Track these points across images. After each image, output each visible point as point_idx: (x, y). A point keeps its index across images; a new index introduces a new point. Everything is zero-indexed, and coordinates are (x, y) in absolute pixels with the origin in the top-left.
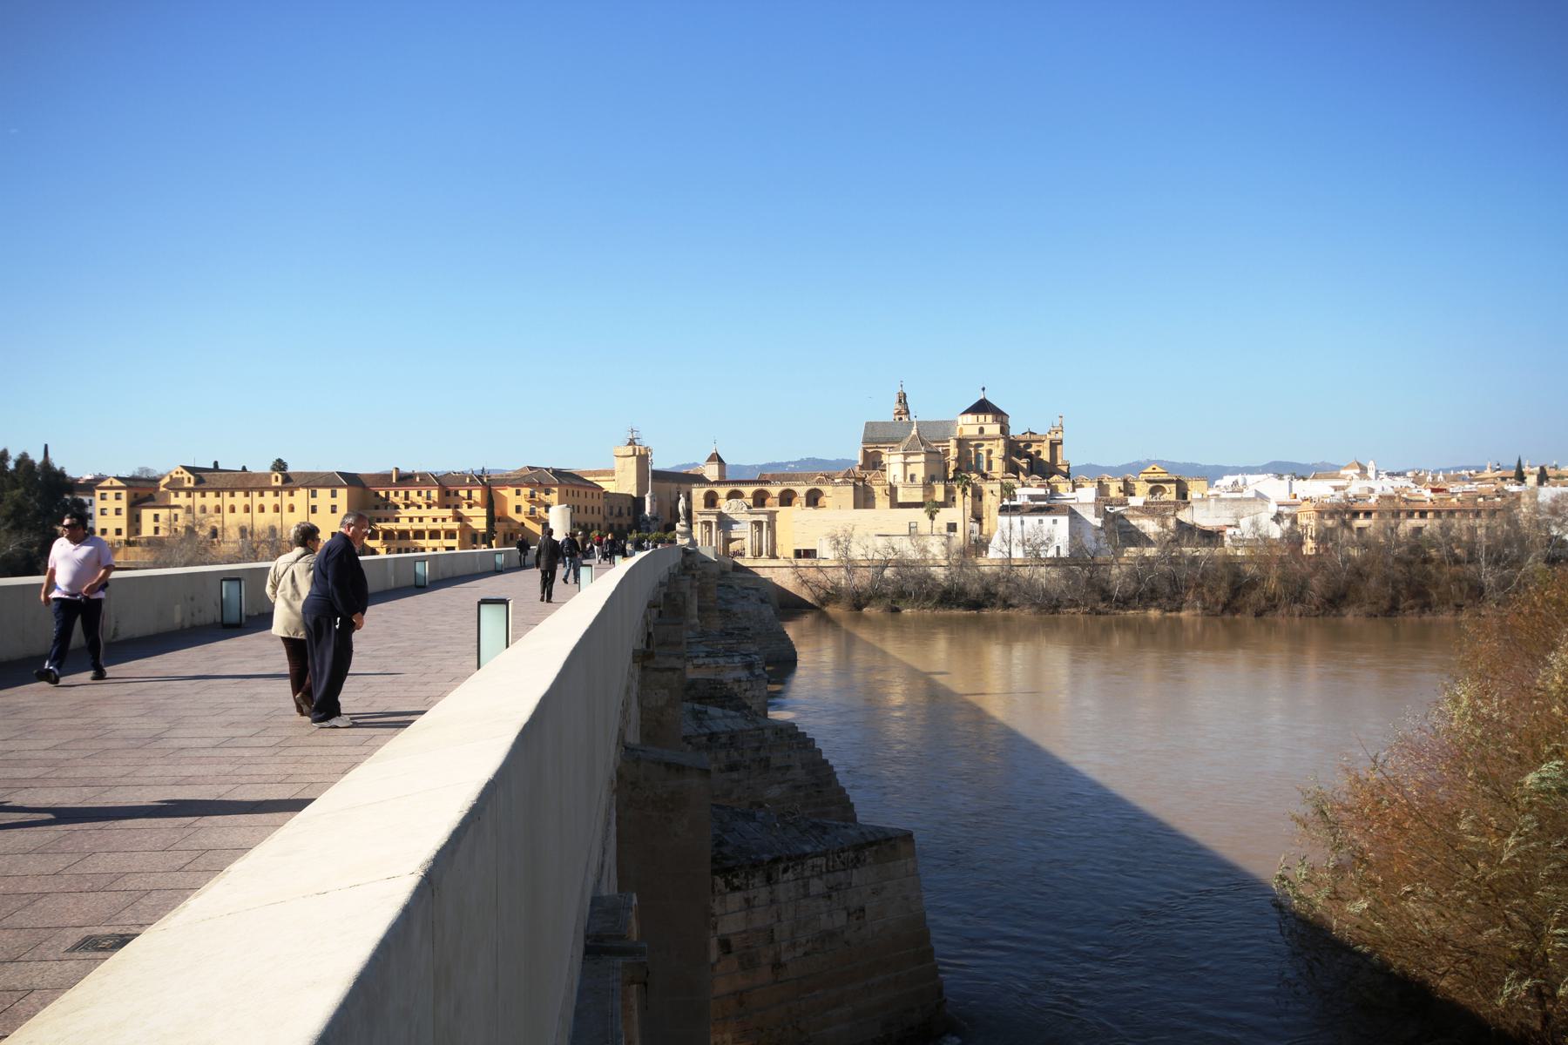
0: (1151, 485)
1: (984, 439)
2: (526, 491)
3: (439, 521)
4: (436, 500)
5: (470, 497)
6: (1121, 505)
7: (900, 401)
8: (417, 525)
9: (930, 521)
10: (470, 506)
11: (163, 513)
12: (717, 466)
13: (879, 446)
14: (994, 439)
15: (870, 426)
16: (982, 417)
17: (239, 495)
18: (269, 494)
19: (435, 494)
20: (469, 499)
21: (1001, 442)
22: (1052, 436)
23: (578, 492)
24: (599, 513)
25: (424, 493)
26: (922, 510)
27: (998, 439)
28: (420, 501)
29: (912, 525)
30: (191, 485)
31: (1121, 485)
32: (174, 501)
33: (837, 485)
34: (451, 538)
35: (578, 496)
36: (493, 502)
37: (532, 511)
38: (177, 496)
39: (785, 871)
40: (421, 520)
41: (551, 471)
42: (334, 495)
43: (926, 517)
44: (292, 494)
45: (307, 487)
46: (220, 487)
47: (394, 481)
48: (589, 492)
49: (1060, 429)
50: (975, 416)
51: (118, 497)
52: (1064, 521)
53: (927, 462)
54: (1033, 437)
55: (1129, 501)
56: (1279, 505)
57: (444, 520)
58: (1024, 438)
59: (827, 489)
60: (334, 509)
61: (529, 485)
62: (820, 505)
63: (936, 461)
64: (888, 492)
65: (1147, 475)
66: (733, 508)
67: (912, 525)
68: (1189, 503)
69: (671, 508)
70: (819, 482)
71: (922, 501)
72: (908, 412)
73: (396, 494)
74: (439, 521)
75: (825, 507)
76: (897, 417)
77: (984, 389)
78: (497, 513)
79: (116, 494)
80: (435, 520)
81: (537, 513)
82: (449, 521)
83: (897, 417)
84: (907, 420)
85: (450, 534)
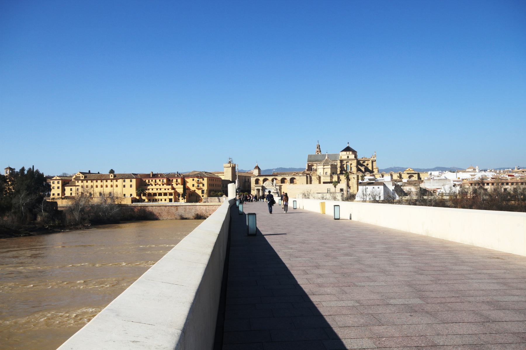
0: (409, 175)
1: (349, 160)
3: (167, 189)
4: (166, 182)
5: (177, 181)
6: (400, 182)
7: (318, 148)
8: (159, 191)
9: (335, 188)
10: (177, 185)
11: (74, 188)
12: (258, 170)
13: (313, 163)
14: (353, 160)
15: (310, 156)
16: (348, 153)
17: (99, 181)
18: (109, 181)
19: (165, 180)
20: (176, 182)
21: (355, 161)
22: (372, 159)
23: (213, 179)
24: (220, 187)
25: (161, 180)
26: (331, 185)
27: (354, 160)
28: (160, 183)
29: (328, 189)
30: (83, 178)
31: (399, 175)
32: (77, 184)
33: (300, 176)
34: (171, 196)
35: (213, 181)
37: (198, 186)
38: (78, 182)
40: (160, 189)
41: (204, 172)
42: (131, 181)
43: (333, 186)
44: (117, 181)
45: (122, 179)
46: (93, 179)
47: (151, 176)
49: (375, 156)
50: (346, 152)
51: (58, 183)
52: (382, 187)
53: (331, 168)
54: (366, 159)
55: (403, 181)
56: (453, 181)
57: (168, 189)
58: (362, 159)
60: (131, 186)
61: (198, 177)
62: (295, 183)
63: (334, 168)
64: (318, 178)
65: (407, 171)
66: (267, 184)
67: (328, 189)
68: (423, 181)
69: (243, 185)
70: (294, 175)
71: (330, 181)
72: (320, 151)
73: (152, 181)
74: (167, 189)
75: (296, 183)
76: (317, 153)
77: (348, 143)
78: (186, 187)
79: (58, 182)
80: (165, 189)
81: (200, 187)
82: (170, 189)
83: (317, 153)
84: (320, 154)
85: (171, 194)
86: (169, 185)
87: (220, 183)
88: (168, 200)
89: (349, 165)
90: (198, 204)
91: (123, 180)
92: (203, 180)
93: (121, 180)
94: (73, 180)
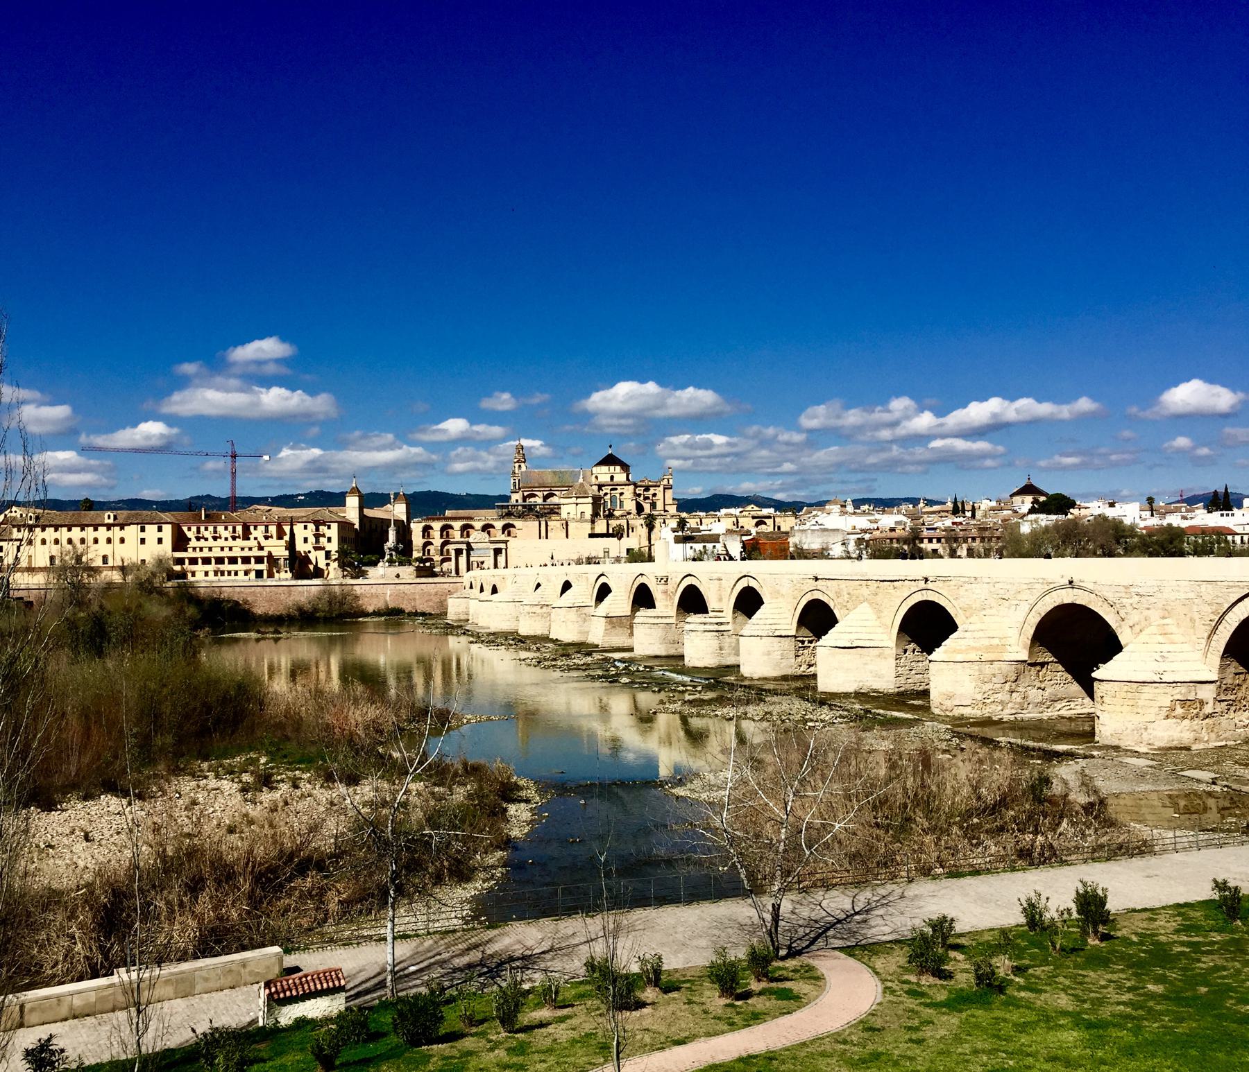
3: (247, 549)
4: (241, 533)
16: (612, 468)
17: (76, 530)
19: (239, 529)
25: (230, 528)
42: (160, 529)
45: (138, 524)
57: (250, 549)
59: (518, 523)
60: (160, 541)
73: (206, 529)
76: (517, 465)
80: (243, 549)
83: (517, 465)
85: (259, 560)
88: (253, 575)
89: (618, 495)
90: (360, 581)
92: (329, 527)
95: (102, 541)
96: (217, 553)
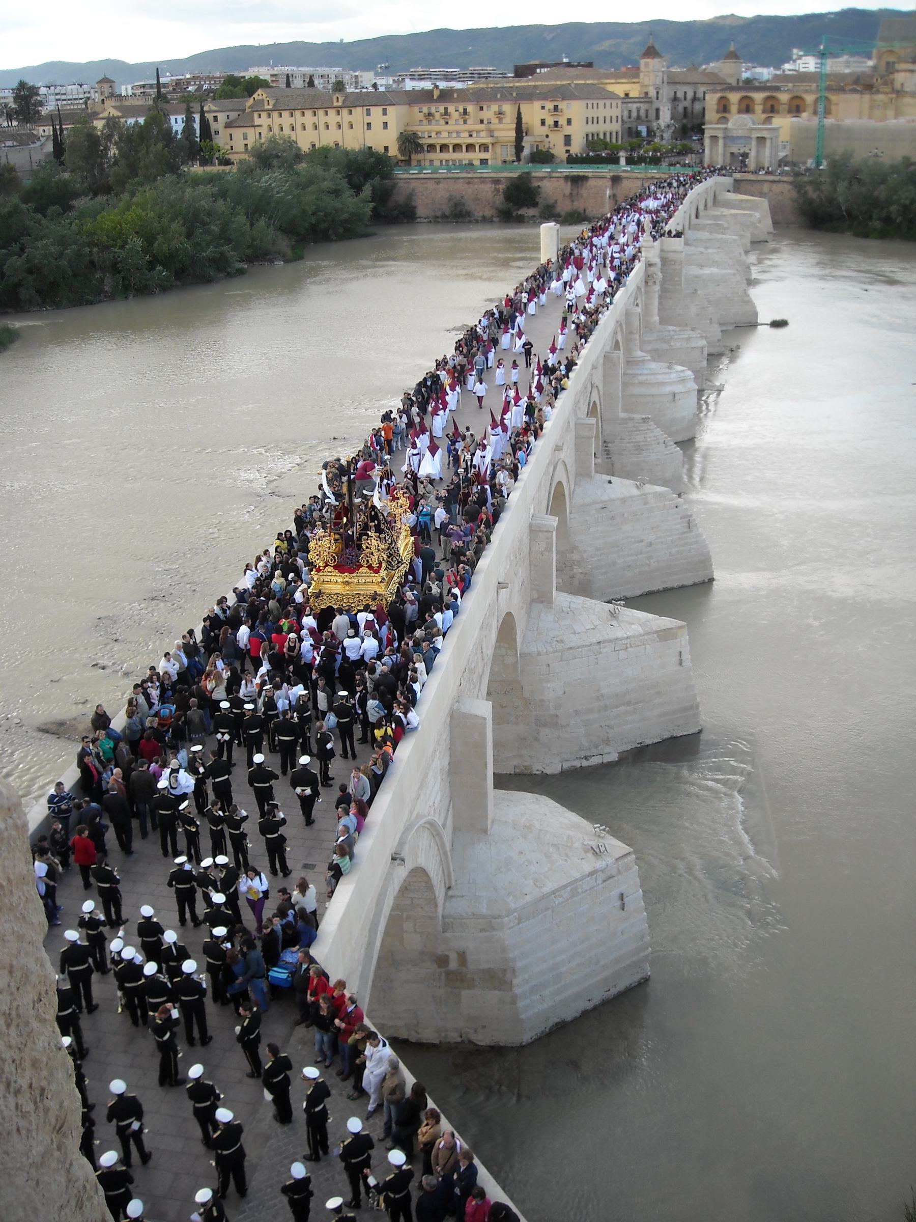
2: (549, 105)
11: (251, 132)
17: (308, 113)
18: (332, 112)
24: (617, 121)
25: (461, 110)
35: (598, 108)
36: (521, 119)
37: (556, 124)
39: (605, 647)
44: (350, 112)
46: (293, 108)
47: (435, 98)
48: (608, 102)
60: (385, 125)
74: (474, 135)
82: (483, 134)
86: (482, 122)
87: (616, 112)
91: (365, 108)
93: (359, 110)
94: (248, 110)
95: (333, 127)
96: (444, 139)
